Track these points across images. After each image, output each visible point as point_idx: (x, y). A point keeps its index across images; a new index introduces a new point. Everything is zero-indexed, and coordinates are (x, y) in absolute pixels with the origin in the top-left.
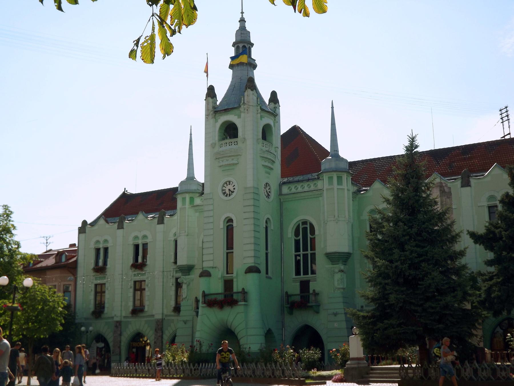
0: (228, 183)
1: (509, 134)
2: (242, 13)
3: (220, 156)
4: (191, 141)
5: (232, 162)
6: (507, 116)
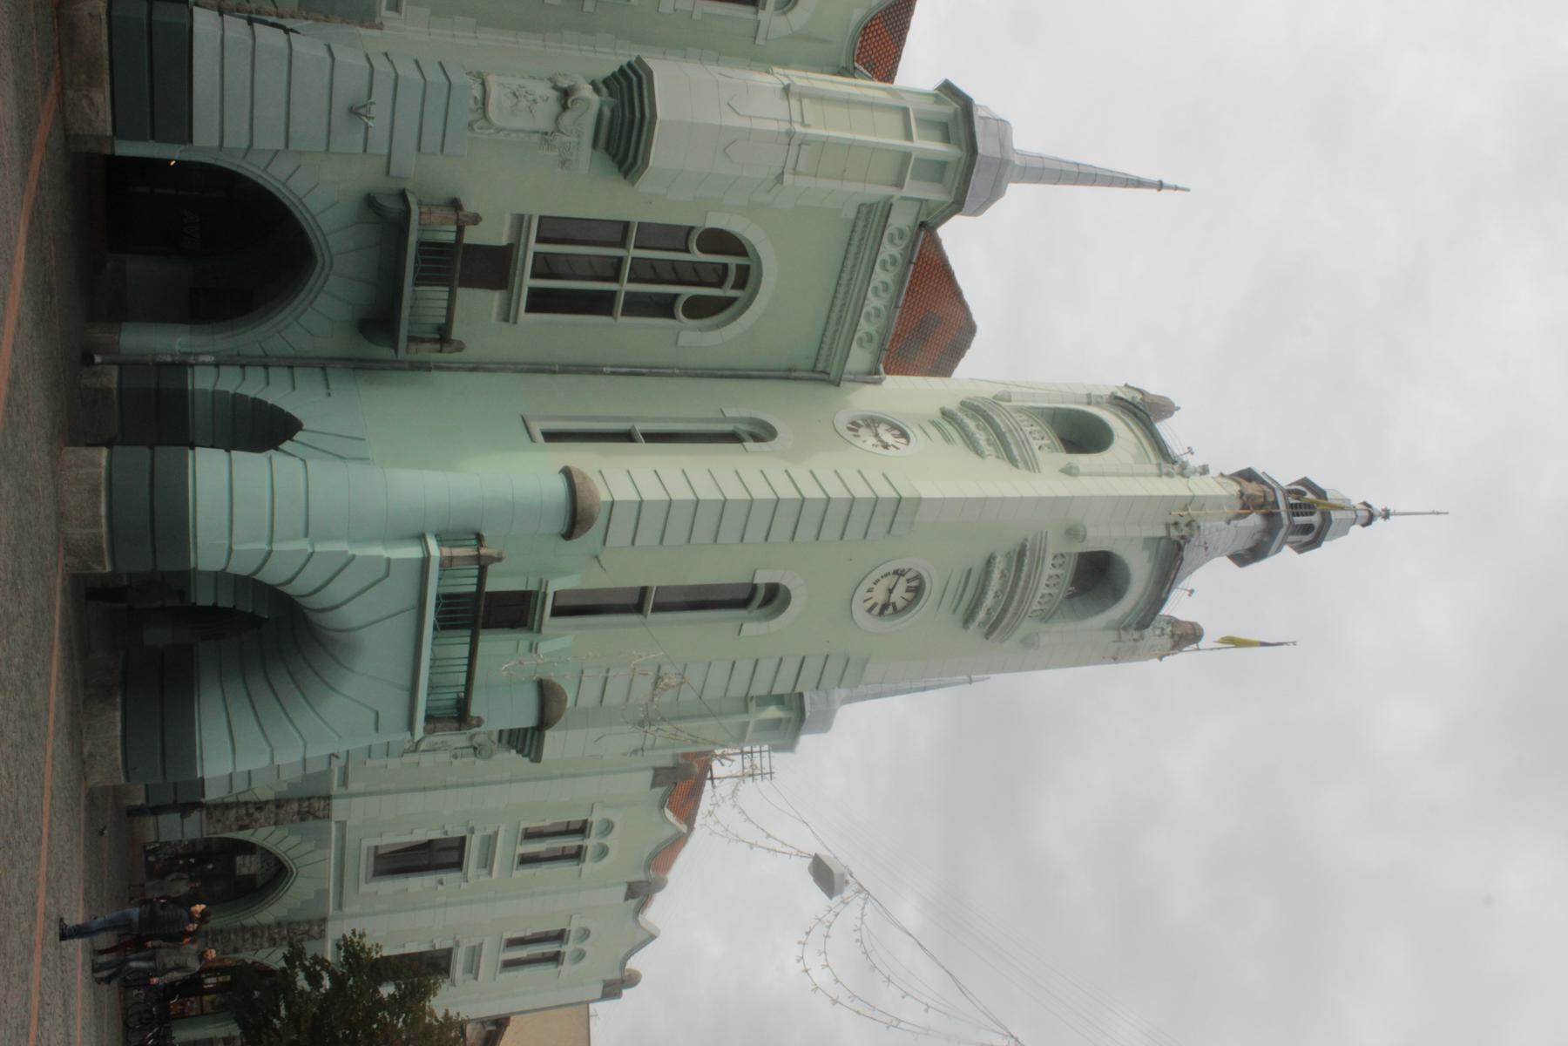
0: (914, 584)
1: (712, 779)
2: (1386, 515)
3: (1025, 569)
4: (1139, 183)
5: (981, 615)
6: (752, 775)
